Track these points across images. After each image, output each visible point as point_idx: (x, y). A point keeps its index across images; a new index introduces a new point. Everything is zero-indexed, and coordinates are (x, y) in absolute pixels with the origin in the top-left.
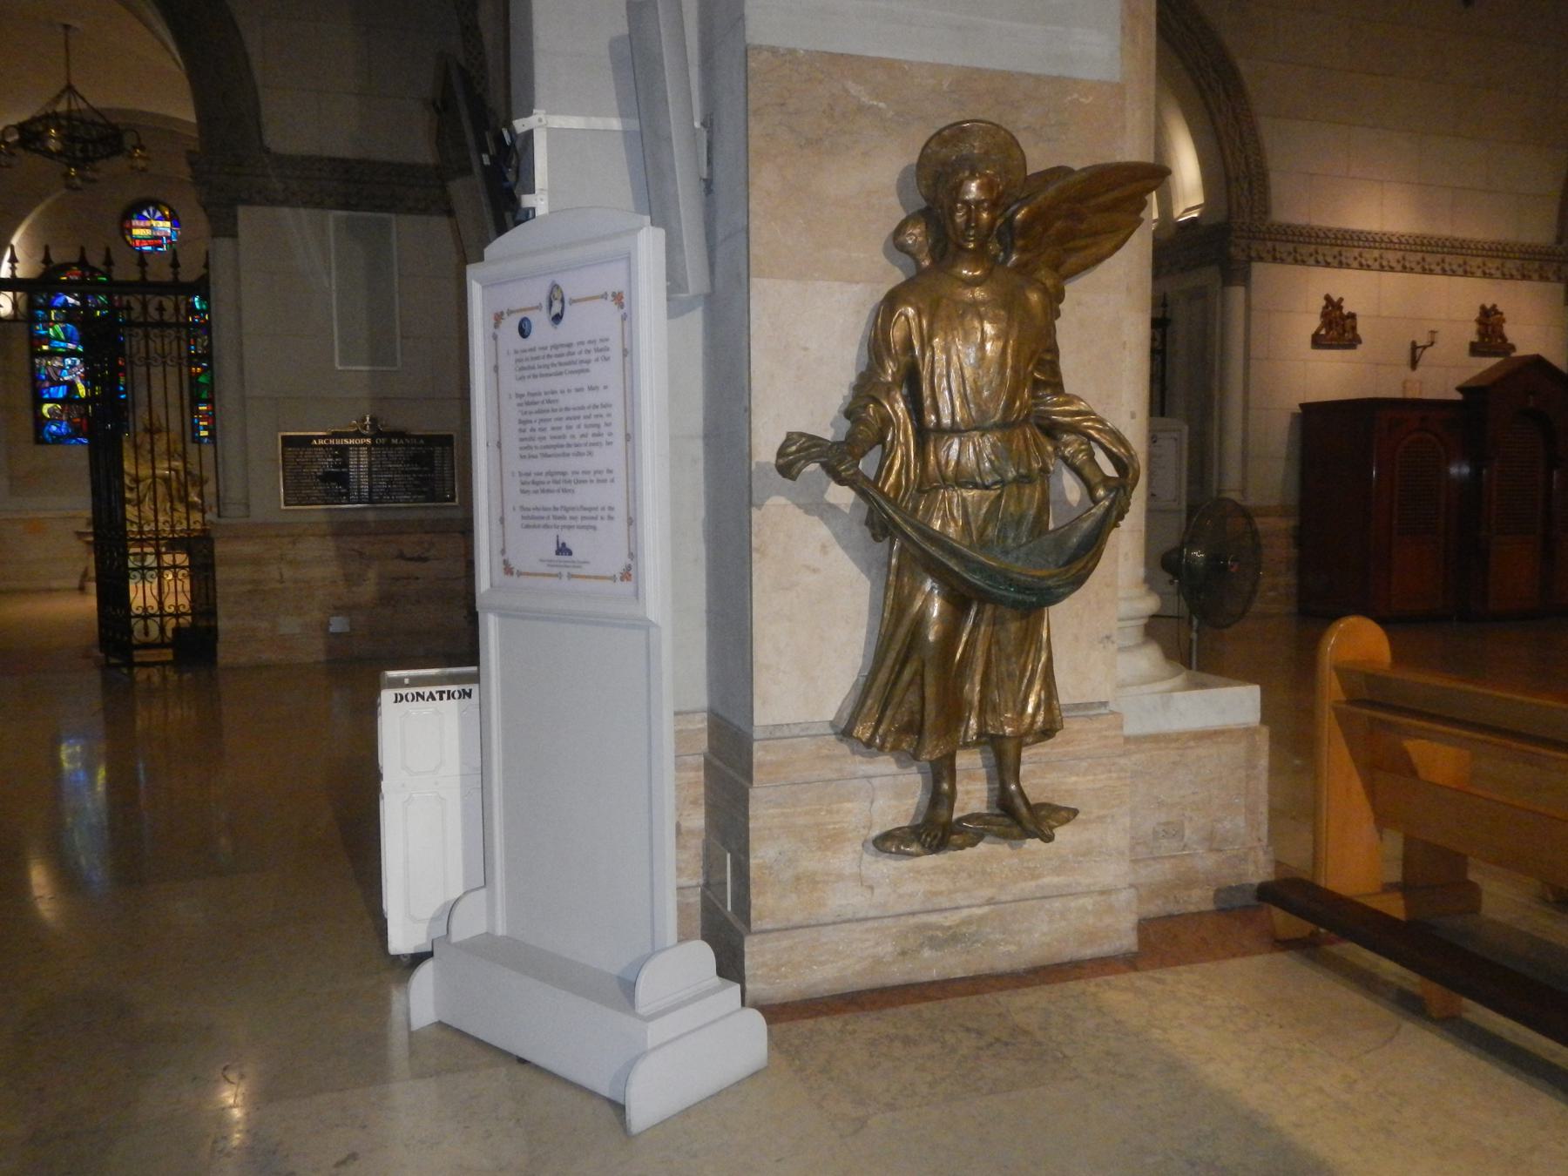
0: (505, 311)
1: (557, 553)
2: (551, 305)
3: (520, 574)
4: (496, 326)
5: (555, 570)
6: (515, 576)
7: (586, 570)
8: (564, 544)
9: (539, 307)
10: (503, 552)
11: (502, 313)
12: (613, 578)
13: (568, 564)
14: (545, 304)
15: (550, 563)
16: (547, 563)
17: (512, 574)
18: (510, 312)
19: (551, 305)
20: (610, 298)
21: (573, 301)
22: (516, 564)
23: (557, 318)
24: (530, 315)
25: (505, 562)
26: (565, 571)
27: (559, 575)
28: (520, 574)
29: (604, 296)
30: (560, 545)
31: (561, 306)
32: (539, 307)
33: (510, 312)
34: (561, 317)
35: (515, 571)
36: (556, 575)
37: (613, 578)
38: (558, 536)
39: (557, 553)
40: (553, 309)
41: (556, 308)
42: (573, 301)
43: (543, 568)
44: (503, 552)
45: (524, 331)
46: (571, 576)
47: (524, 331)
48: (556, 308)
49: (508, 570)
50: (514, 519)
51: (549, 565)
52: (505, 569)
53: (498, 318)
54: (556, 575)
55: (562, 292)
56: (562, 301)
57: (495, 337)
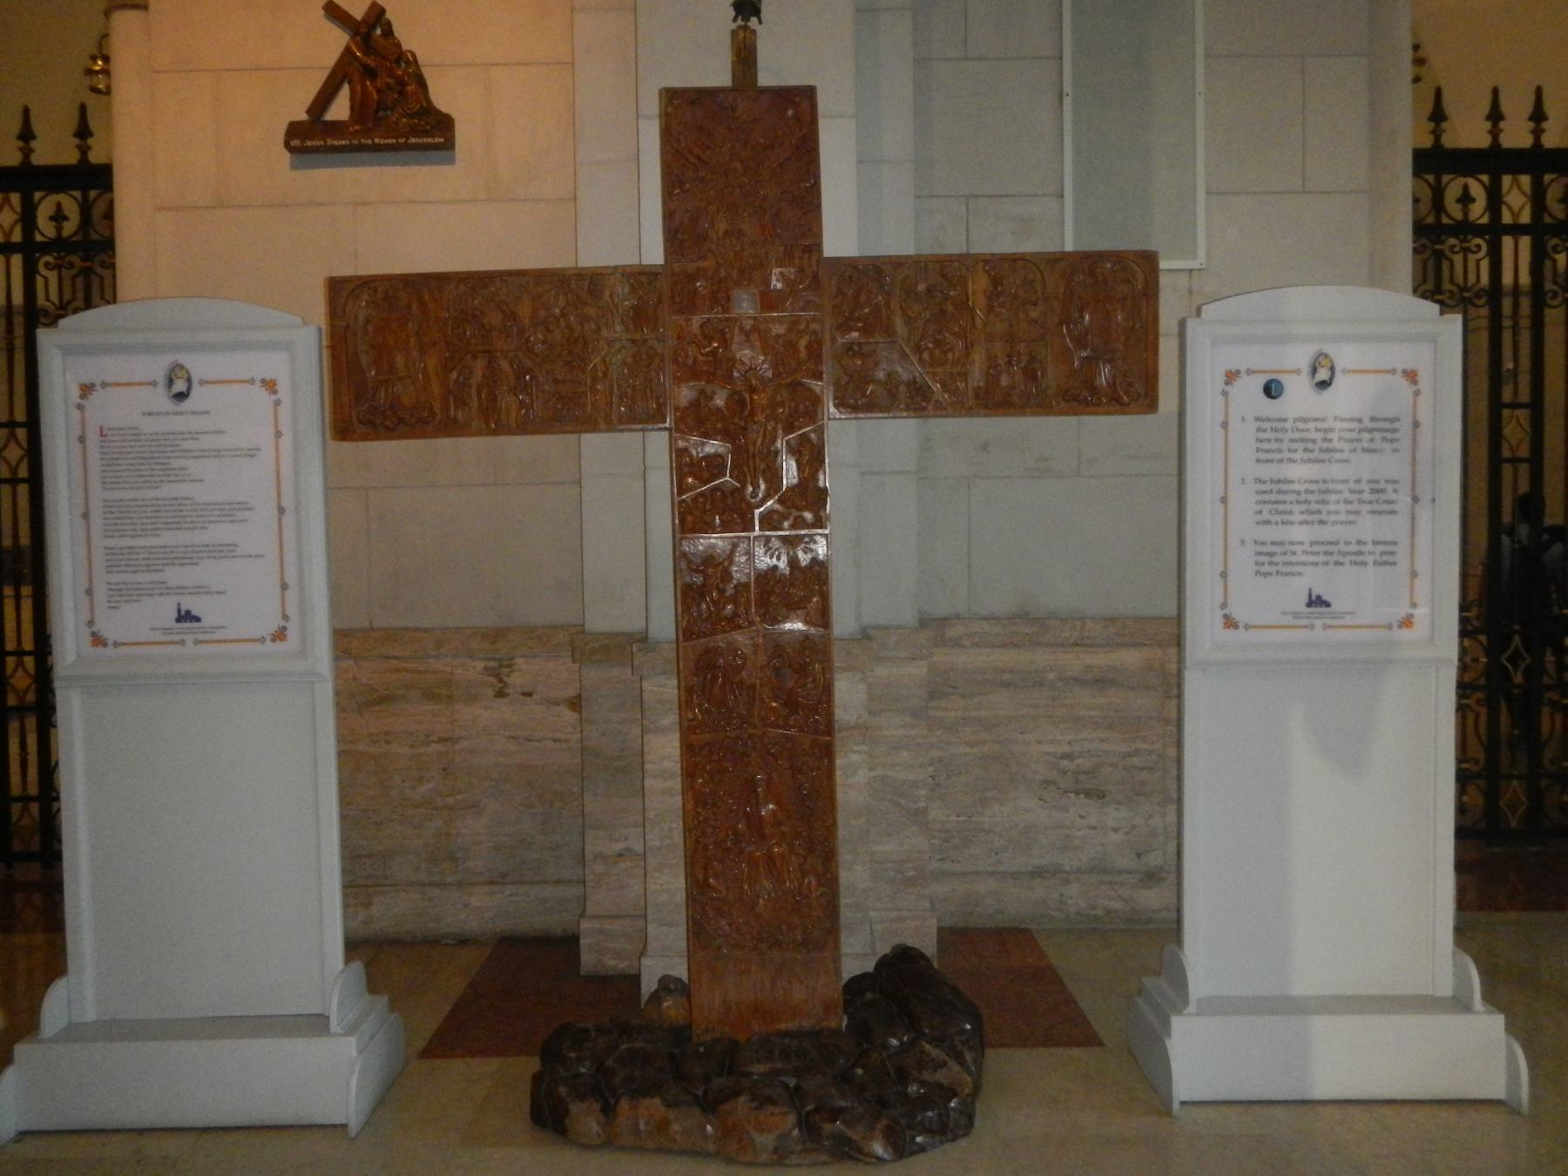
2: (1314, 371)
3: (1247, 627)
4: (1227, 383)
5: (1305, 622)
9: (1298, 372)
10: (1224, 605)
11: (1238, 372)
18: (1249, 372)
19: (1314, 371)
23: (1324, 385)
24: (1287, 380)
27: (1311, 627)
32: (1298, 372)
33: (1249, 372)
35: (1241, 625)
41: (1323, 375)
44: (1224, 605)
45: (1271, 390)
47: (1271, 390)
49: (1230, 623)
50: (101, 594)
52: (1225, 624)
53: (1231, 377)
56: (1332, 369)
57: (1225, 394)
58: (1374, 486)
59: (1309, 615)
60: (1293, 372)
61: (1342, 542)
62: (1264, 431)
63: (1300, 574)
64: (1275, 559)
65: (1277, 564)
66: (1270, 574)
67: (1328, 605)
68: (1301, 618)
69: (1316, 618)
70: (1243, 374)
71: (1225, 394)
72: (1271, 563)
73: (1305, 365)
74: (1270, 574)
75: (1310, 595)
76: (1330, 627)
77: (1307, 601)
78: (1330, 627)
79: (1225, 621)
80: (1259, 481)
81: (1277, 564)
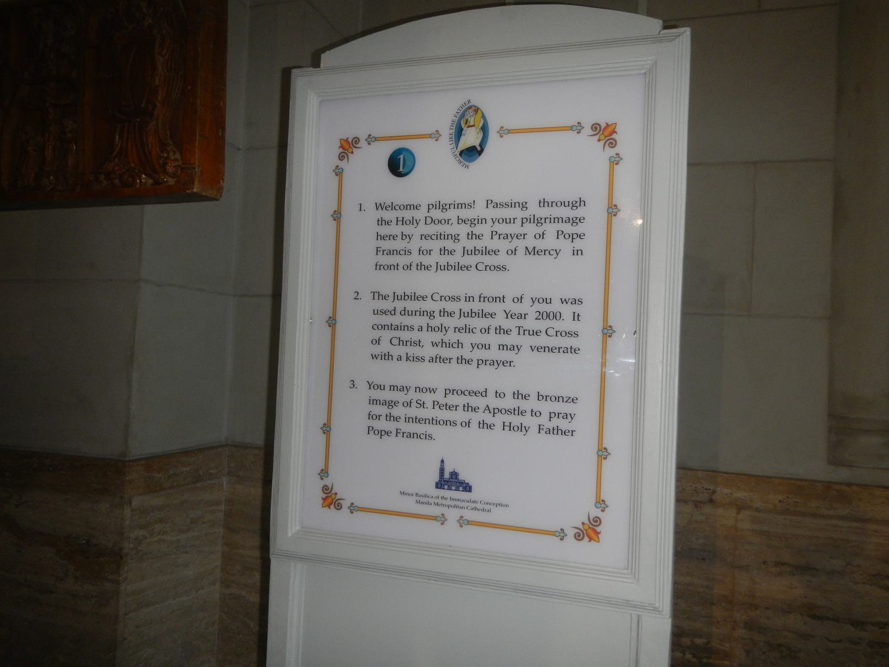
0: (363, 137)
1: (439, 485)
2: (459, 133)
3: (353, 508)
4: (341, 157)
6: (345, 510)
7: (497, 516)
8: (454, 475)
9: (435, 136)
10: (324, 473)
11: (356, 140)
12: (561, 535)
13: (458, 503)
14: (446, 131)
15: (421, 498)
16: (415, 498)
17: (339, 507)
18: (371, 139)
19: (459, 133)
20: (587, 131)
21: (503, 132)
22: (341, 490)
23: (472, 153)
25: (325, 489)
26: (453, 515)
28: (353, 508)
29: (578, 128)
30: (447, 476)
31: (481, 136)
32: (435, 136)
33: (371, 139)
34: (480, 153)
35: (345, 504)
36: (435, 518)
37: (561, 535)
38: (442, 461)
39: (439, 485)
40: (463, 138)
41: (471, 138)
42: (503, 132)
43: (409, 505)
44: (324, 473)
46: (463, 522)
48: (471, 138)
49: (331, 500)
51: (418, 502)
52: (324, 499)
53: (348, 147)
54: (435, 518)
55: (483, 117)
56: (484, 129)
57: (339, 172)
58: (544, 308)
59: (440, 501)
60: (429, 136)
61: (491, 393)
62: (388, 223)
63: (429, 437)
64: (397, 411)
65: (396, 419)
66: (388, 433)
67: (468, 488)
68: (428, 503)
69: (449, 506)
70: (363, 143)
71: (339, 172)
72: (389, 417)
73: (445, 125)
74: (388, 433)
75: (442, 471)
76: (469, 523)
77: (437, 478)
78: (469, 523)
79: (324, 496)
80: (377, 295)
81: (396, 419)
